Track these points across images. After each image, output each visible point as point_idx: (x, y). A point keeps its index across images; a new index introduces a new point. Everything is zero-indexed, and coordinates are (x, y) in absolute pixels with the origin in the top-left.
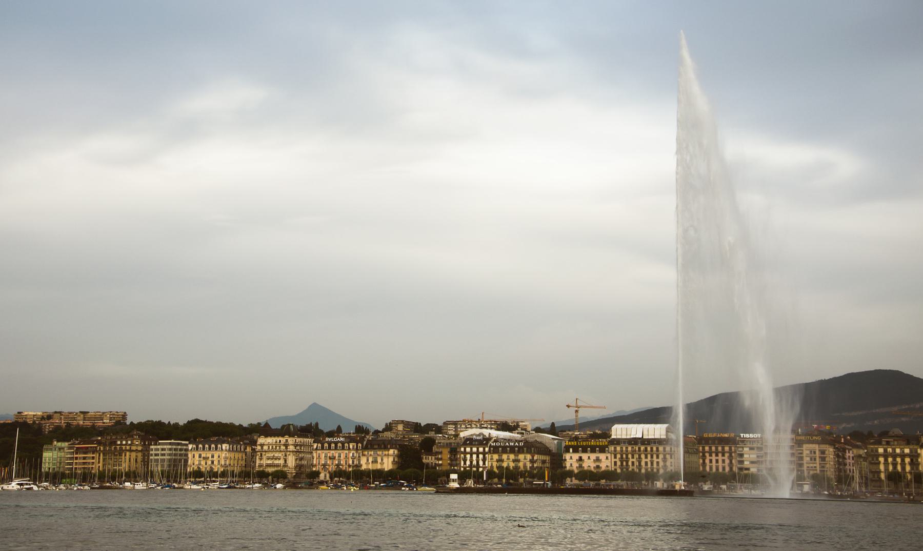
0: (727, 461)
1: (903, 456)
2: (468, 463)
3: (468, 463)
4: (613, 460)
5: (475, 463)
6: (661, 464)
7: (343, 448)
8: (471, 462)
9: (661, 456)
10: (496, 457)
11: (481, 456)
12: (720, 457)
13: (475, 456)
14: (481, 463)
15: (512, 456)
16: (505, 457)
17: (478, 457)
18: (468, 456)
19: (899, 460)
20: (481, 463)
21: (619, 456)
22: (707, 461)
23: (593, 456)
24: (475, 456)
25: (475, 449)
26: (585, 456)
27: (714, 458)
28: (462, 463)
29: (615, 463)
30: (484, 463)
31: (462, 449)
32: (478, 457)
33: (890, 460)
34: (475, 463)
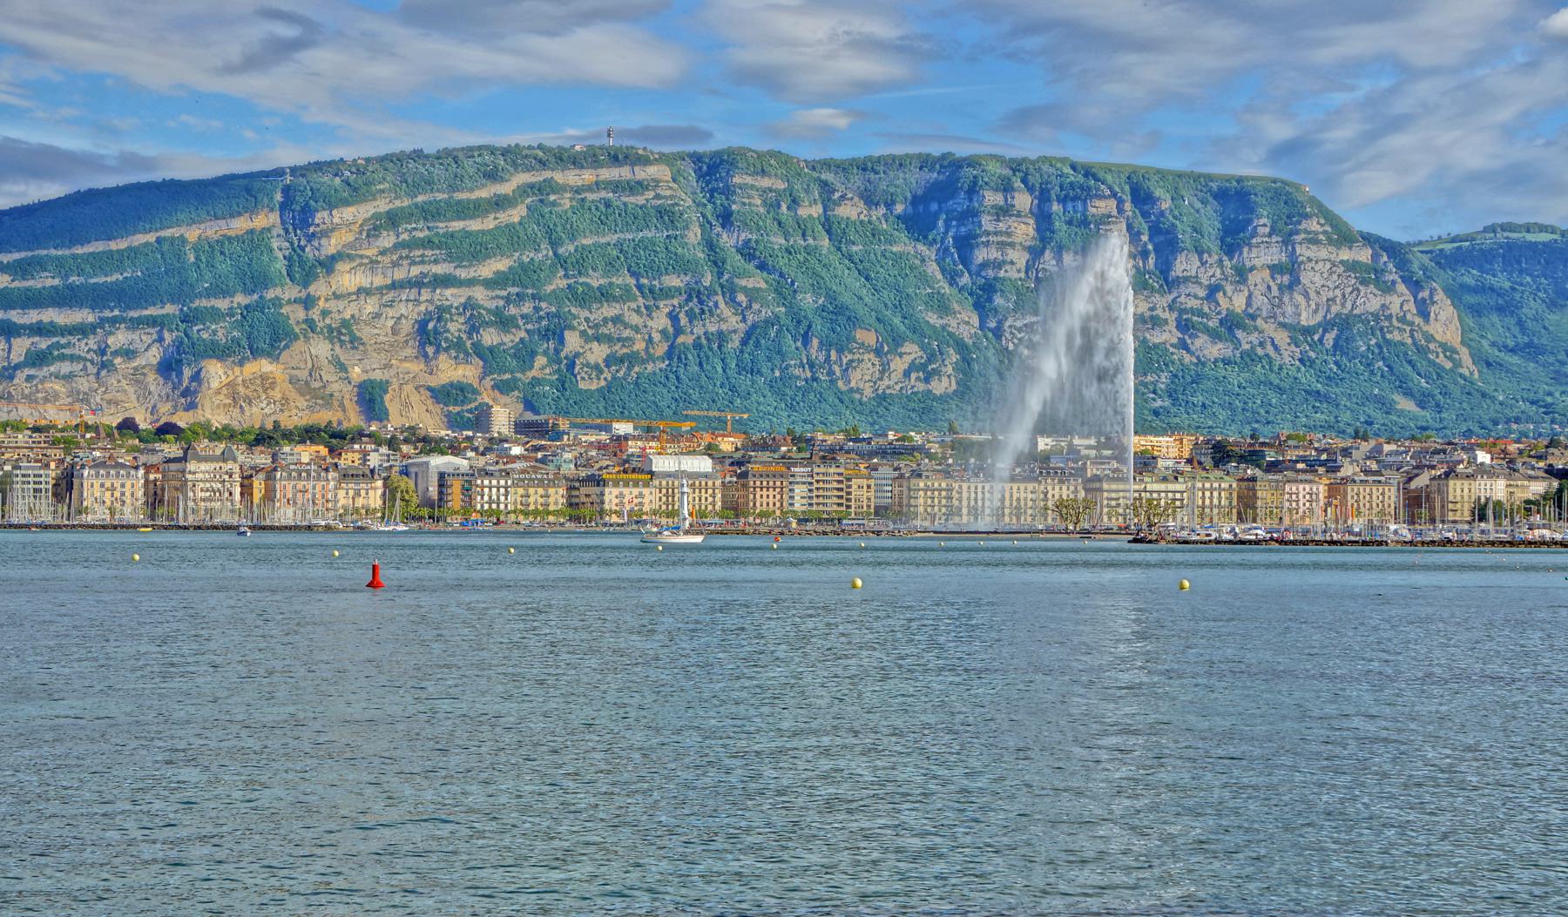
0: (778, 497)
1: (940, 490)
4: (658, 495)
5: (494, 497)
6: (710, 499)
9: (710, 491)
10: (521, 491)
11: (502, 490)
12: (771, 492)
13: (494, 490)
14: (502, 498)
15: (541, 491)
16: (531, 491)
19: (936, 493)
20: (502, 498)
21: (664, 491)
22: (758, 496)
23: (636, 491)
24: (494, 490)
26: (626, 491)
27: (765, 492)
29: (660, 499)
31: (479, 482)
33: (929, 493)
34: (494, 497)
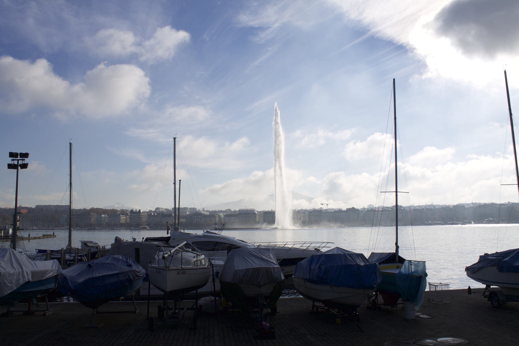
2: (196, 221)
3: (196, 221)
5: (198, 220)
7: (157, 217)
8: (197, 220)
11: (200, 219)
13: (198, 219)
17: (199, 219)
18: (196, 219)
20: (200, 221)
24: (198, 219)
25: (198, 217)
28: (194, 221)
30: (201, 221)
32: (199, 219)
34: (198, 220)
